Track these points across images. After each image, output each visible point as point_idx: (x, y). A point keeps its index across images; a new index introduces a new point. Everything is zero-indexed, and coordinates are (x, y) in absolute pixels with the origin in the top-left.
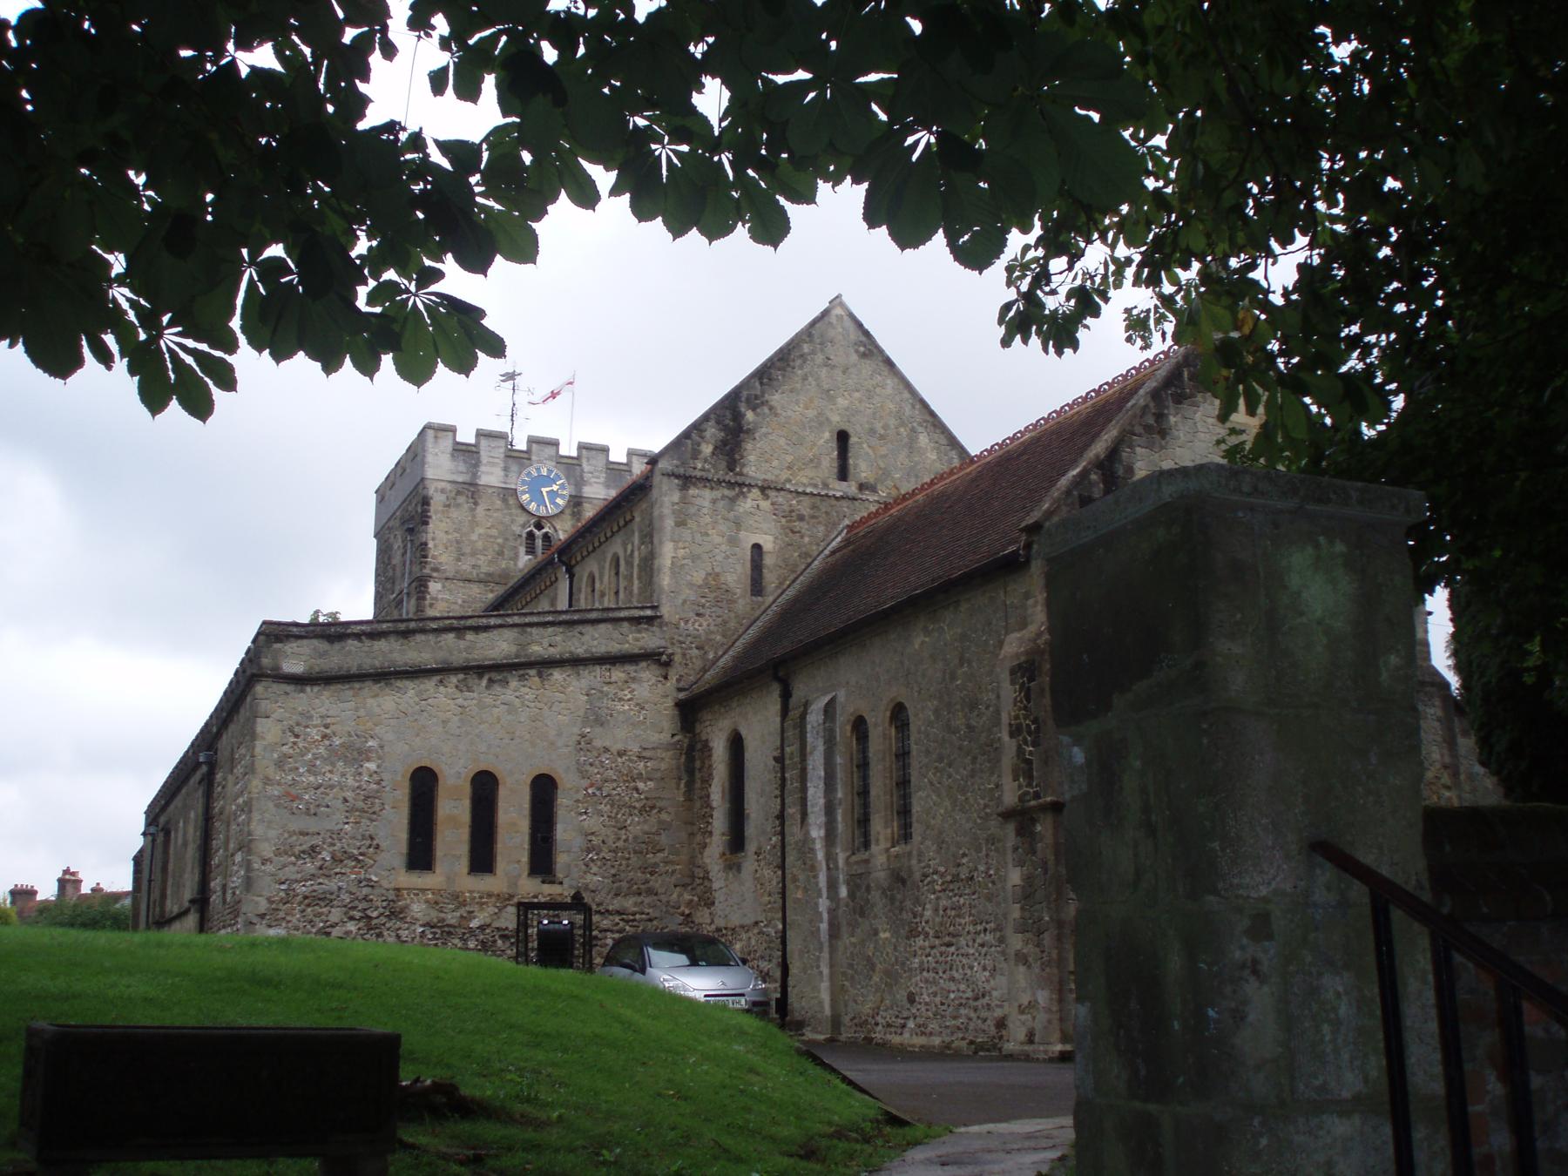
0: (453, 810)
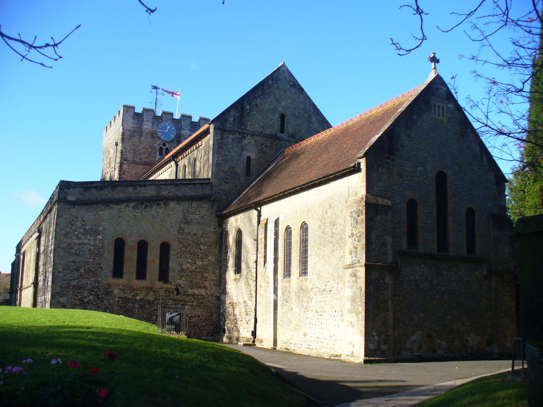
0: (131, 255)
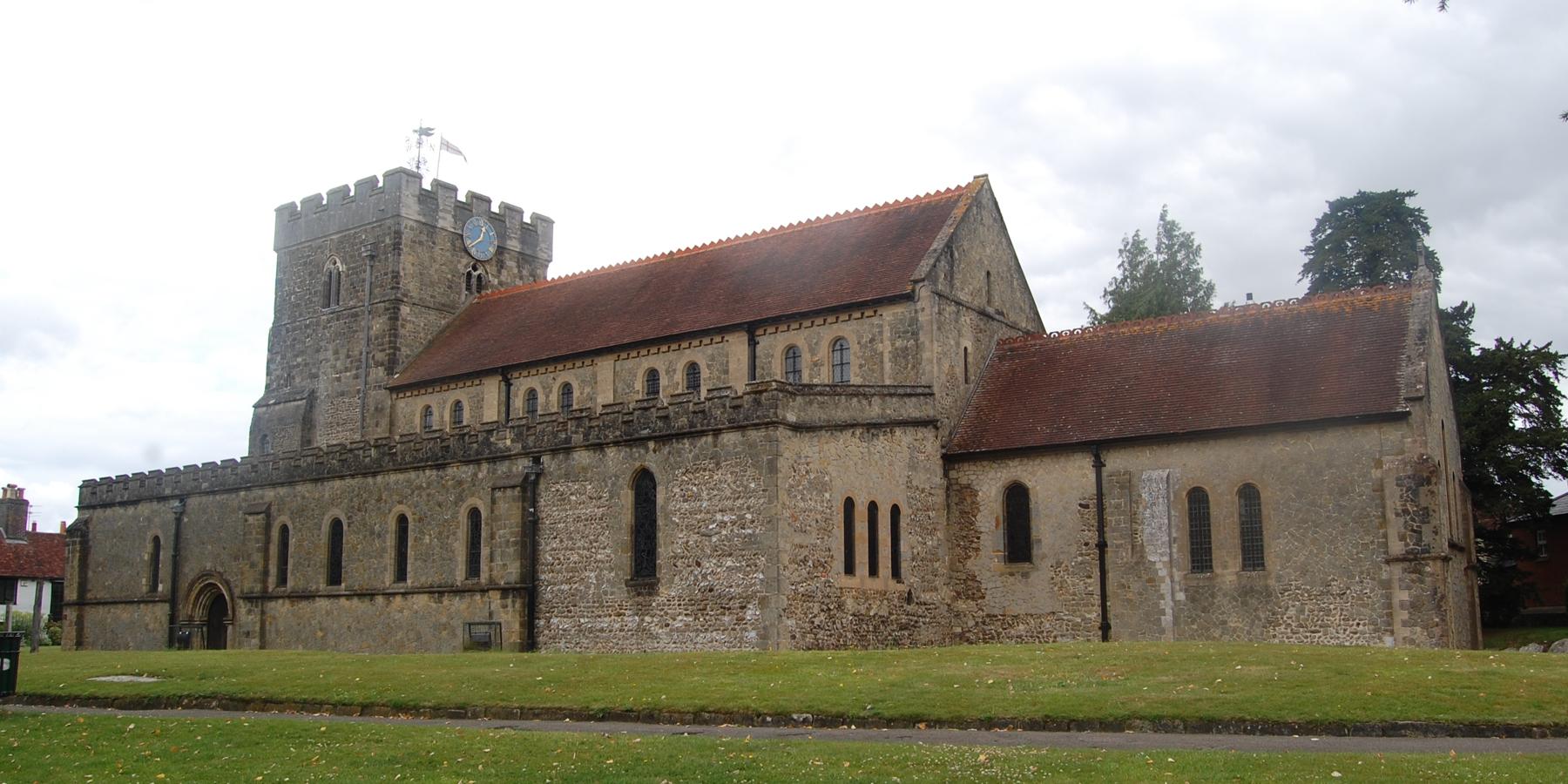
0: (861, 528)
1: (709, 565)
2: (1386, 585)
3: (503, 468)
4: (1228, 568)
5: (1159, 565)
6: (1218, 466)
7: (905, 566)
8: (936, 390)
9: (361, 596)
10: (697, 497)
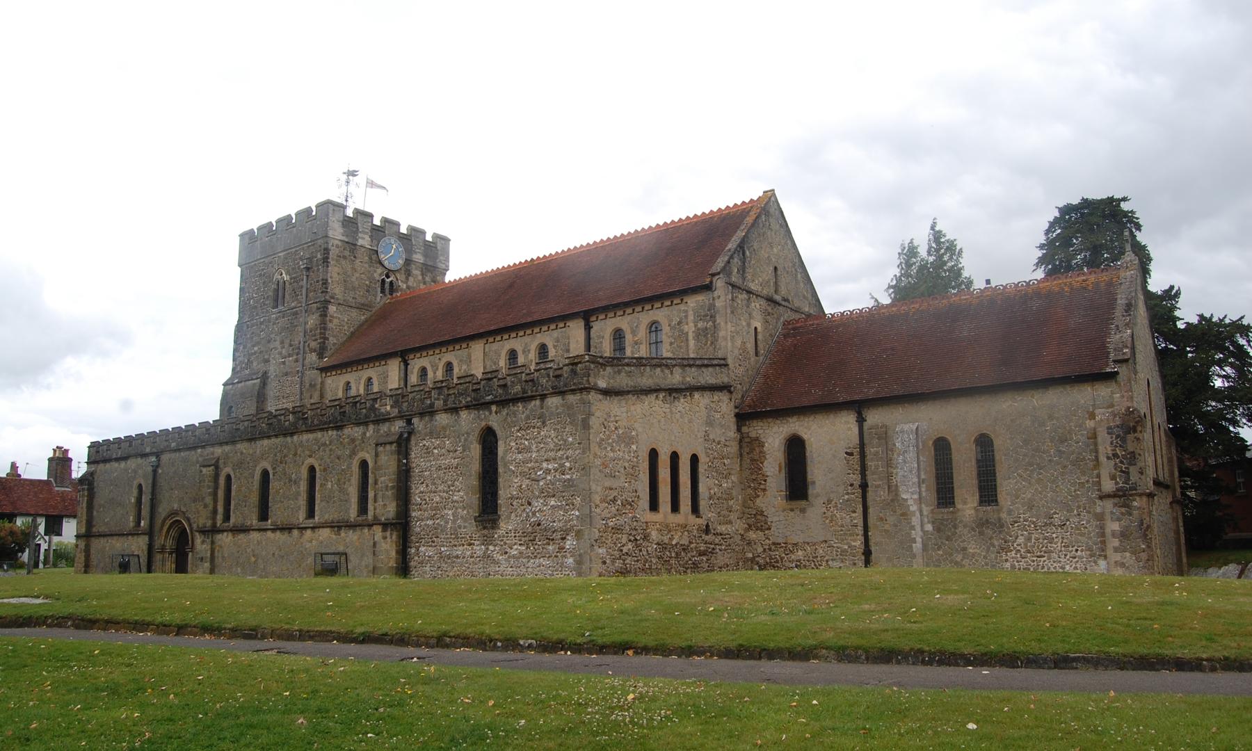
0: (664, 474)
1: (537, 504)
2: (1100, 517)
3: (384, 428)
4: (967, 504)
5: (910, 502)
6: (959, 419)
7: (703, 504)
8: (730, 361)
9: (282, 529)
10: (528, 450)
